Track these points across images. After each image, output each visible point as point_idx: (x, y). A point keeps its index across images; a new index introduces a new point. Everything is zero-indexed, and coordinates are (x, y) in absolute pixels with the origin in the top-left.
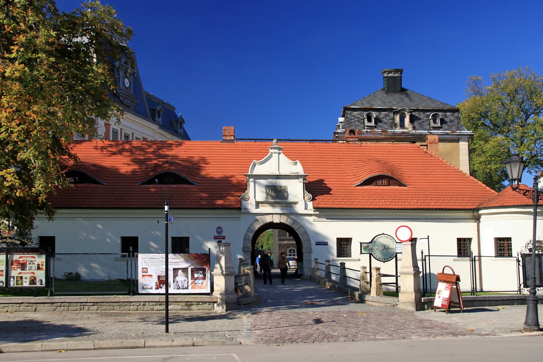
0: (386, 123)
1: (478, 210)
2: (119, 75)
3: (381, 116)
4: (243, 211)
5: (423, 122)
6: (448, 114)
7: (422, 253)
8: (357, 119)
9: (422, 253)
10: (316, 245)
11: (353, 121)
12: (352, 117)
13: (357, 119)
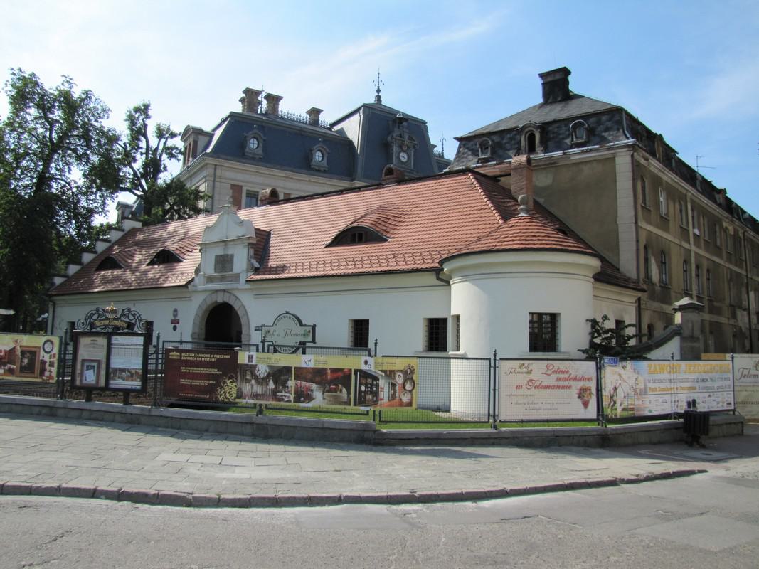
2: (393, 150)
3: (504, 141)
6: (604, 118)
7: (158, 338)
9: (158, 338)
10: (256, 330)
11: (465, 156)
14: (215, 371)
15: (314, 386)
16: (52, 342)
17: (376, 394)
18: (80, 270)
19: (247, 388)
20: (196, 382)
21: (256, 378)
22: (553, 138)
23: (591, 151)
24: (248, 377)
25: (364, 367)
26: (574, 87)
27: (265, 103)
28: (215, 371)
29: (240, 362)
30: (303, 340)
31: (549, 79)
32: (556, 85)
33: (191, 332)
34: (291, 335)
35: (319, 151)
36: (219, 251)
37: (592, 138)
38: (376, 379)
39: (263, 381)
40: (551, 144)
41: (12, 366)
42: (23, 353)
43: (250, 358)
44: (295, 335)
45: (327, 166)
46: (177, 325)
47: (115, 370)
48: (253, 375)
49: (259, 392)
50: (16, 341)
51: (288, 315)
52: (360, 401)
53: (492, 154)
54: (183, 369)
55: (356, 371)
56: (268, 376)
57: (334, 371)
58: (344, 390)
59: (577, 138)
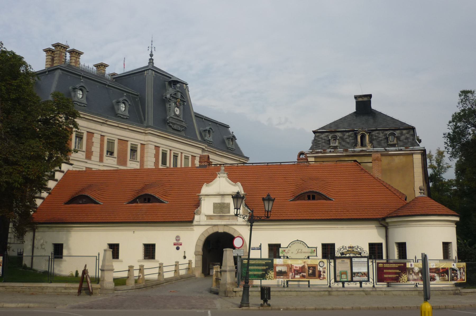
0: (348, 143)
1: (384, 219)
3: (345, 137)
4: (195, 223)
5: (382, 140)
6: (404, 132)
8: (323, 141)
11: (320, 142)
12: (320, 139)
13: (323, 141)
14: (398, 271)
15: (436, 275)
16: (323, 262)
17: (457, 276)
18: (42, 203)
19: (411, 277)
20: (390, 276)
21: (414, 273)
22: (376, 139)
23: (401, 150)
24: (411, 273)
25: (453, 267)
26: (375, 106)
27: (68, 55)
28: (398, 271)
29: (407, 267)
30: (310, 255)
31: (360, 99)
32: (363, 103)
33: (194, 251)
34: (301, 252)
35: (124, 103)
36: (218, 200)
37: (399, 142)
38: (457, 271)
39: (417, 274)
40: (374, 142)
41: (304, 274)
42: (309, 268)
43: (411, 265)
44: (304, 252)
45: (128, 115)
46: (179, 246)
47: (355, 273)
48: (413, 271)
49: (416, 278)
50: (305, 262)
51: (299, 242)
52: (452, 279)
53: (340, 143)
54: (385, 271)
55: (450, 268)
56: (419, 271)
57: (442, 268)
58: (447, 276)
59: (391, 141)
